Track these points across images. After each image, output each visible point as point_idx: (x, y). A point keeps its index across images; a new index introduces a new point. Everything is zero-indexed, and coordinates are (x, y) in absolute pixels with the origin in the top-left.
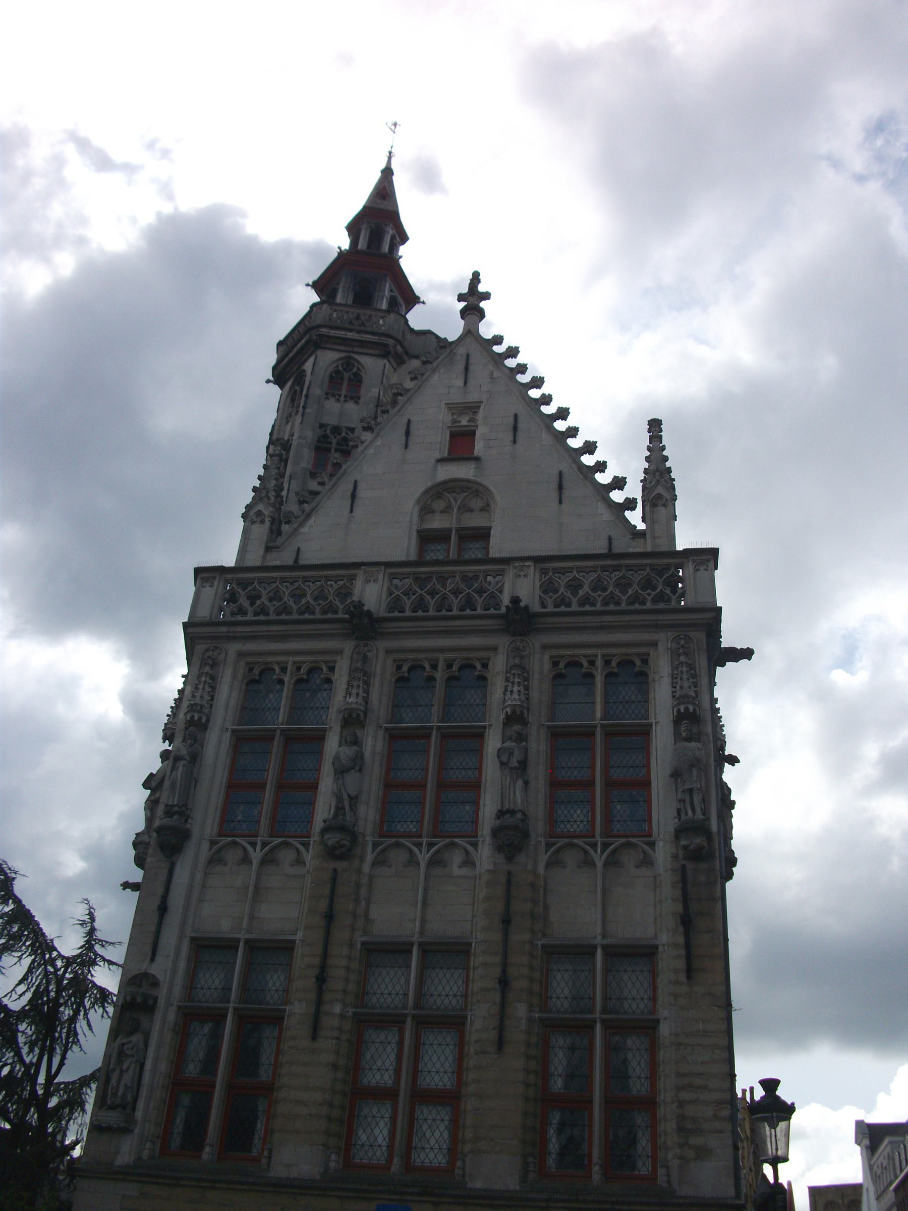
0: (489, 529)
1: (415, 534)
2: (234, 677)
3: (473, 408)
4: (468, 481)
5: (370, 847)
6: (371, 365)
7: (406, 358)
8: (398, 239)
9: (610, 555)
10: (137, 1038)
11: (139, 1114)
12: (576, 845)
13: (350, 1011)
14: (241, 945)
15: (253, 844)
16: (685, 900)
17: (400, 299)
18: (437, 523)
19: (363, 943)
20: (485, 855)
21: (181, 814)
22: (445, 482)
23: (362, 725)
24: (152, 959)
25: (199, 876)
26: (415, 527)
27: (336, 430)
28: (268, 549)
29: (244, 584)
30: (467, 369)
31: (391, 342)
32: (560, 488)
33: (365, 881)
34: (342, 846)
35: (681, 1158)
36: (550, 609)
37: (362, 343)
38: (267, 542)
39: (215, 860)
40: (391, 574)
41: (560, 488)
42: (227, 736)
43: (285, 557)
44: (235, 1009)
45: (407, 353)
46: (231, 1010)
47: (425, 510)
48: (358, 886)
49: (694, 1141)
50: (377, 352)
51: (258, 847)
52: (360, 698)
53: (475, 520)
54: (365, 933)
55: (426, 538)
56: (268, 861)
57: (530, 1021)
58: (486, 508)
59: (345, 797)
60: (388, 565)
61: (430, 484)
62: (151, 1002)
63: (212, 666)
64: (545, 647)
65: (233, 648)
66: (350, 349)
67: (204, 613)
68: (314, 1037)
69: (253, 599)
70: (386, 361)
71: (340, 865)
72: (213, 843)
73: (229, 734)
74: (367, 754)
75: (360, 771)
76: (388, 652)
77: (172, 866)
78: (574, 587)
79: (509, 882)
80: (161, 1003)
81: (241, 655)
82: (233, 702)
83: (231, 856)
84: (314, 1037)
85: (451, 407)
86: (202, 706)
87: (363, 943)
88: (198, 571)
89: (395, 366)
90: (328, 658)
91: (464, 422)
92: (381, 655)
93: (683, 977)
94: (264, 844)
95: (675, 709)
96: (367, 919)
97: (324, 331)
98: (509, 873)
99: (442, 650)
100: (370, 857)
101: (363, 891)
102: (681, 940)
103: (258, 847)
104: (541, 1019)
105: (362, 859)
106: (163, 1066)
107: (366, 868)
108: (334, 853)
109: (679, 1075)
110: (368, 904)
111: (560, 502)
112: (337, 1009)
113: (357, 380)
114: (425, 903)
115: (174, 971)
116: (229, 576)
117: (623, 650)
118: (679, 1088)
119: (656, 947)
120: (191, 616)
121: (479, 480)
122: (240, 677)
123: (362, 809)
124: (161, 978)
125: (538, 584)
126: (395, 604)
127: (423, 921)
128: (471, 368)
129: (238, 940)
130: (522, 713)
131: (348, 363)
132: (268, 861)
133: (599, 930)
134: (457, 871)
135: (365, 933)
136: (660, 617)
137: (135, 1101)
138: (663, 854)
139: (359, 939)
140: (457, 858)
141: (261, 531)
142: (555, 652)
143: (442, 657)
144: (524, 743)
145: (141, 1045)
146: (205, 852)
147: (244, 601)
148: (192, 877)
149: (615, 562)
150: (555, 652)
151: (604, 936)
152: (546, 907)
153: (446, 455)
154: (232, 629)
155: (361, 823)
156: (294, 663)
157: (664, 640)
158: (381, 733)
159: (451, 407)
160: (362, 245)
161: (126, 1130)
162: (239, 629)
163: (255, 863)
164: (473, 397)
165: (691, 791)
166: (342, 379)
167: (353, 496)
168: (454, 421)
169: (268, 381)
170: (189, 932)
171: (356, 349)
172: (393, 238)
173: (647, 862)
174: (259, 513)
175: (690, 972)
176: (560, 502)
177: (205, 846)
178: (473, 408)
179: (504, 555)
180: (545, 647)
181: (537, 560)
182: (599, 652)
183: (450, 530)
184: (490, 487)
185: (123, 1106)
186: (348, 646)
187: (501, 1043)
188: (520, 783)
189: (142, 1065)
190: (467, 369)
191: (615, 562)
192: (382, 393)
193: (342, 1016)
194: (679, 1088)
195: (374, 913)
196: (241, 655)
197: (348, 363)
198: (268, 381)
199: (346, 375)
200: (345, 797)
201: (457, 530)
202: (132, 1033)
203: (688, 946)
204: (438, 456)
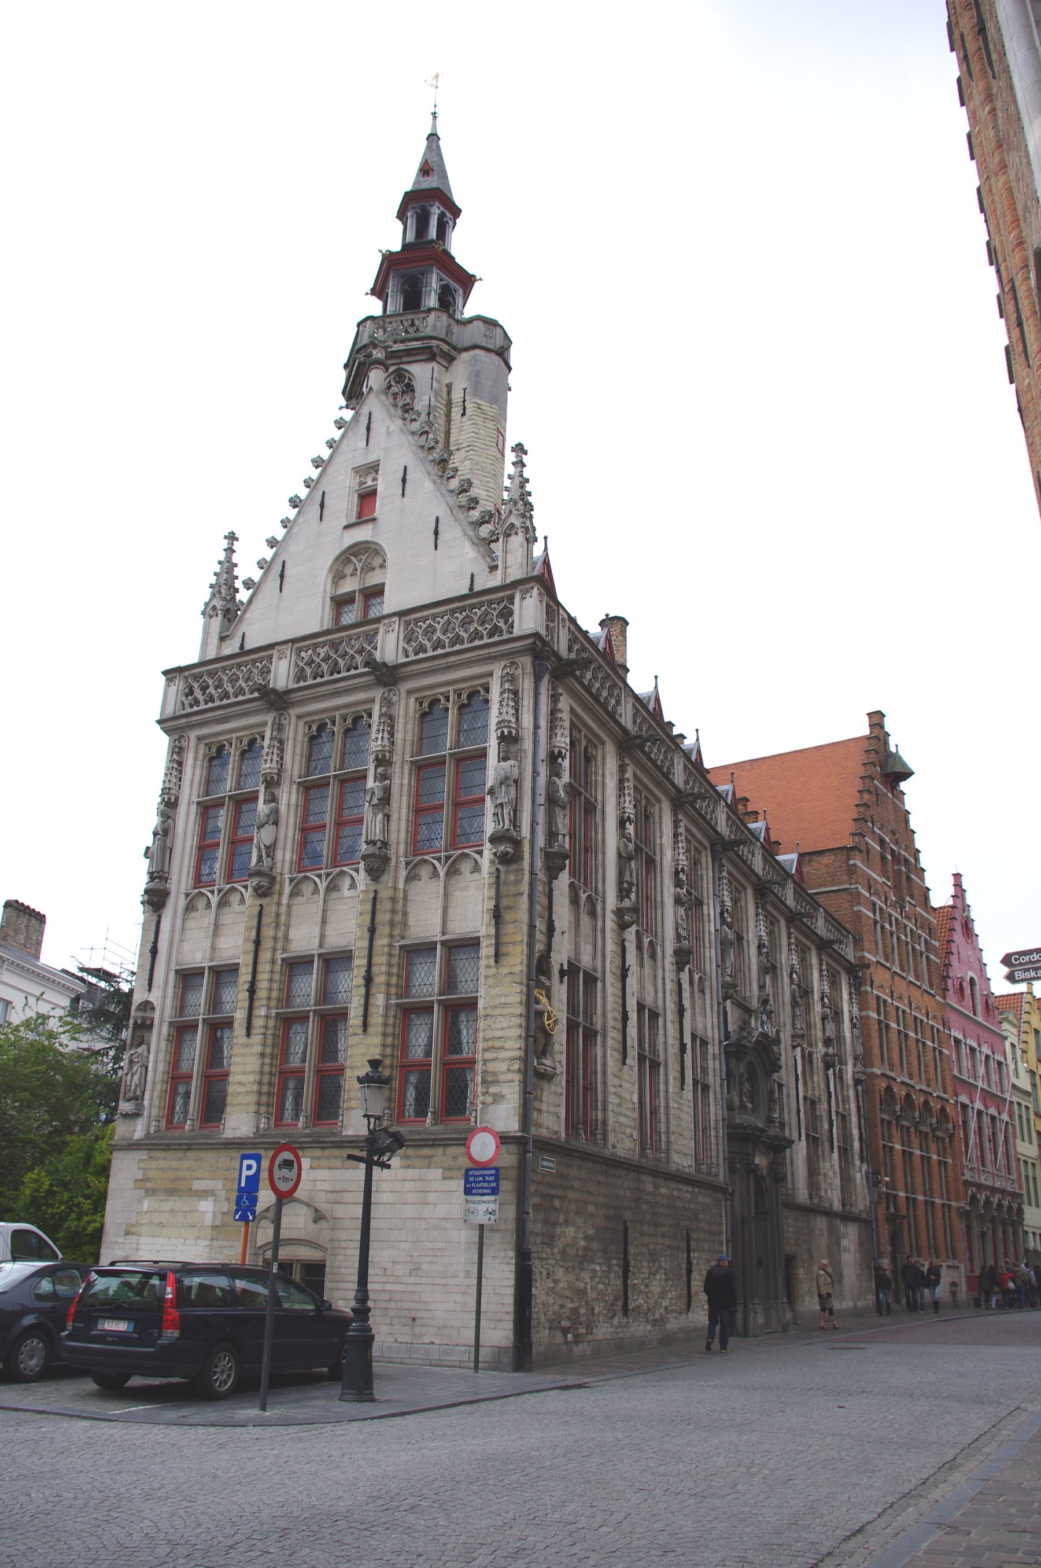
0: (383, 584)
1: (328, 601)
2: (196, 759)
3: (373, 468)
4: (368, 542)
5: (287, 882)
7: (454, 353)
8: (448, 215)
9: (472, 594)
10: (144, 1047)
11: (146, 1103)
12: (426, 861)
13: (274, 1012)
14: (206, 971)
15: (212, 892)
16: (498, 897)
17: (454, 285)
19: (283, 960)
20: (362, 878)
21: (160, 878)
22: (351, 547)
23: (278, 784)
24: (150, 991)
25: (179, 922)
26: (328, 595)
28: (222, 639)
29: (197, 677)
30: (368, 429)
31: (434, 343)
32: (436, 533)
33: (283, 909)
34: (262, 887)
35: (483, 1103)
36: (412, 658)
37: (409, 352)
38: (221, 633)
39: (190, 908)
40: (297, 648)
41: (436, 533)
42: (194, 808)
43: (231, 648)
44: (204, 1020)
45: (455, 348)
46: (201, 1021)
47: (338, 576)
48: (278, 915)
49: (493, 1089)
50: (424, 357)
51: (216, 893)
52: (274, 762)
53: (373, 579)
54: (284, 950)
55: (340, 602)
56: (223, 903)
57: (387, 1007)
59: (262, 847)
60: (293, 641)
61: (338, 552)
62: (148, 1022)
63: (178, 753)
64: (409, 692)
65: (193, 735)
66: (398, 361)
67: (170, 711)
68: (248, 1035)
69: (204, 689)
70: (434, 364)
71: (265, 901)
72: (187, 895)
73: (195, 806)
74: (283, 808)
75: (276, 823)
76: (299, 717)
77: (160, 917)
78: (430, 631)
79: (375, 899)
80: (156, 1021)
81: (200, 739)
82: (197, 779)
83: (201, 903)
84: (248, 1035)
85: (357, 470)
86: (169, 789)
87: (283, 960)
88: (166, 673)
89: (446, 365)
90: (259, 730)
91: (370, 483)
92: (293, 720)
93: (492, 961)
94: (220, 891)
95: (499, 731)
96: (286, 938)
98: (375, 891)
99: (337, 708)
100: (287, 889)
101: (283, 919)
102: (493, 931)
103: (216, 893)
104: (397, 1005)
105: (280, 894)
106: (161, 1067)
107: (285, 900)
108: (262, 892)
109: (486, 1040)
110: (288, 926)
111: (436, 548)
112: (263, 1012)
114: (324, 921)
115: (164, 996)
116: (187, 673)
117: (469, 684)
118: (485, 1050)
119: (478, 938)
120: (162, 713)
121: (375, 540)
122: (201, 757)
123: (279, 854)
124: (155, 1003)
125: (402, 636)
126: (301, 676)
127: (322, 936)
128: (372, 426)
129: (204, 968)
130: (384, 756)
132: (223, 903)
133: (439, 929)
134: (346, 893)
135: (284, 950)
136: (491, 650)
137: (143, 1093)
138: (486, 860)
139: (279, 956)
140: (347, 882)
141: (217, 622)
142: (418, 695)
143: (337, 714)
144: (388, 782)
145: (145, 1054)
146: (182, 902)
147: (198, 693)
148: (174, 924)
149: (461, 604)
150: (418, 695)
151: (444, 933)
152: (405, 914)
153: (354, 520)
154: (189, 719)
155: (279, 865)
156: (237, 738)
157: (497, 669)
158: (295, 788)
159: (357, 470)
160: (411, 237)
161: (137, 1115)
162: (194, 718)
163: (214, 906)
164: (372, 458)
165: (501, 804)
167: (282, 576)
168: (361, 484)
169: (341, 408)
170: (174, 967)
171: (404, 360)
172: (442, 216)
173: (476, 868)
174: (214, 608)
175: (497, 956)
176: (436, 548)
177: (182, 897)
178: (373, 468)
180: (409, 692)
182: (451, 688)
183: (355, 592)
184: (384, 545)
185: (136, 1098)
186: (269, 718)
187: (365, 1026)
188: (380, 816)
189: (147, 1068)
190: (368, 429)
191: (461, 604)
192: (433, 399)
193: (267, 1017)
194: (485, 1050)
195: (292, 936)
196: (200, 739)
197: (400, 376)
198: (341, 408)
200: (262, 847)
201: (360, 591)
202: (139, 1046)
203: (497, 936)
204: (345, 523)
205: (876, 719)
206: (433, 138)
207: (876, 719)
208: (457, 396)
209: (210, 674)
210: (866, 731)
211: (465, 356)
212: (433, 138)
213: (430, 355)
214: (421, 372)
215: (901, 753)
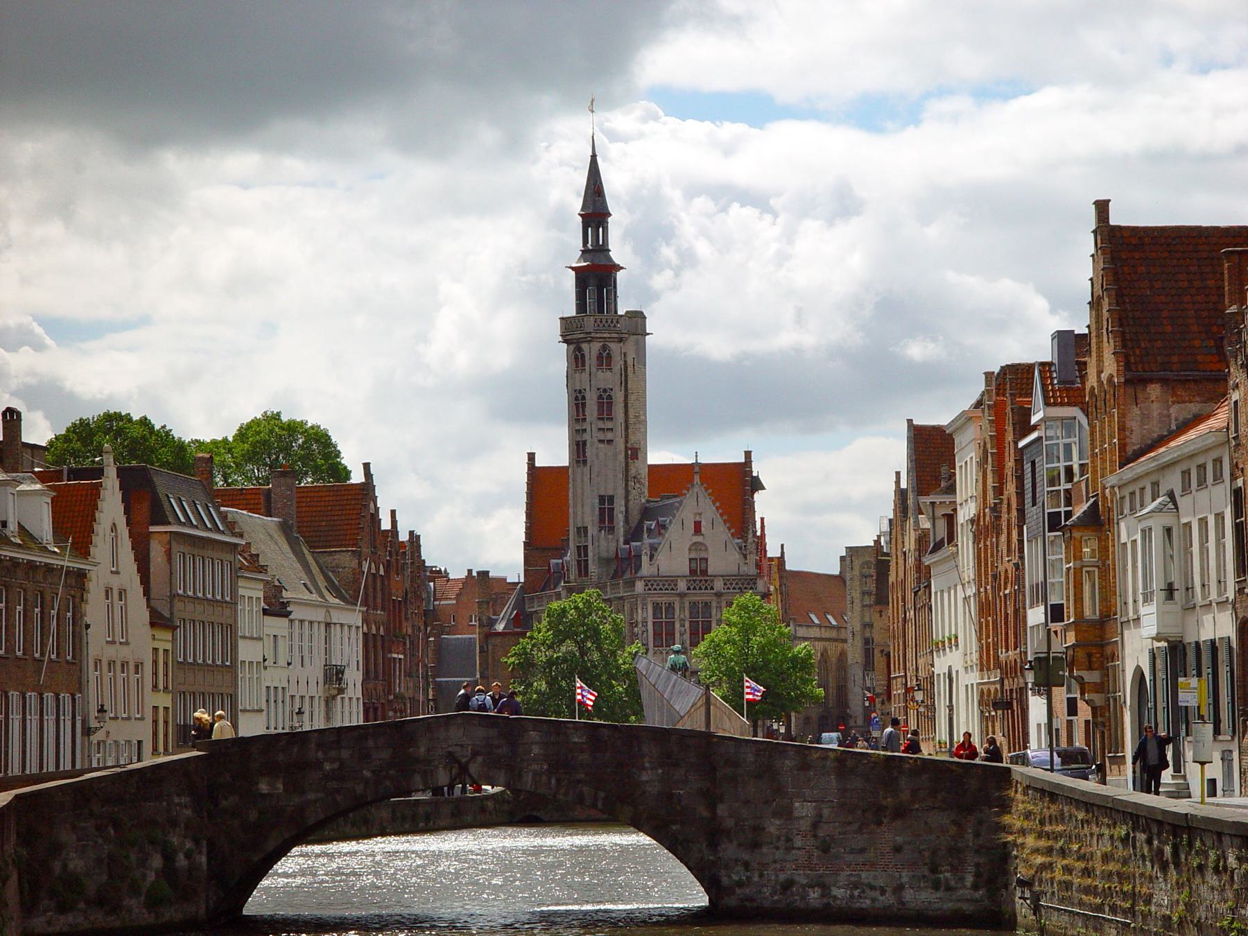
6: (613, 346)
18: (693, 556)
27: (605, 391)
29: (649, 581)
47: (690, 550)
53: (703, 555)
58: (706, 550)
65: (649, 599)
97: (593, 335)
113: (609, 357)
126: (689, 589)
131: (604, 348)
166: (603, 357)
178: (700, 514)
179: (714, 574)
181: (722, 576)
199: (605, 355)
205: (748, 454)
206: (594, 157)
207: (748, 454)
208: (630, 362)
209: (655, 581)
210: (743, 461)
211: (633, 338)
212: (594, 157)
213: (620, 340)
214: (613, 346)
215: (760, 477)
